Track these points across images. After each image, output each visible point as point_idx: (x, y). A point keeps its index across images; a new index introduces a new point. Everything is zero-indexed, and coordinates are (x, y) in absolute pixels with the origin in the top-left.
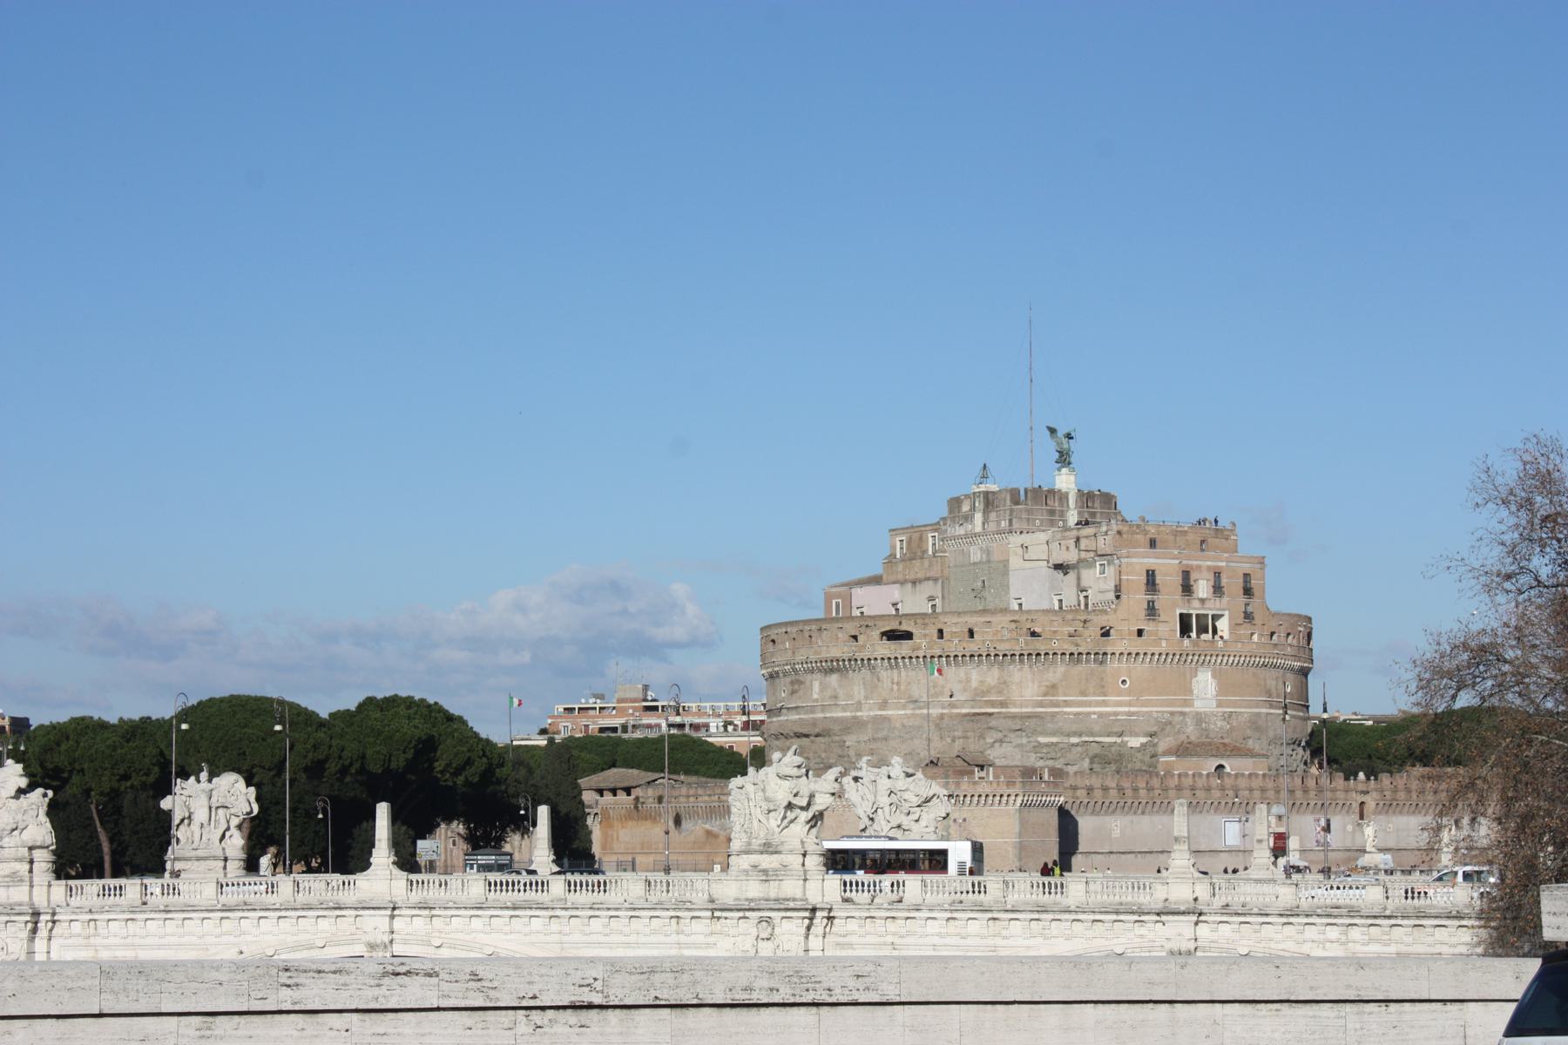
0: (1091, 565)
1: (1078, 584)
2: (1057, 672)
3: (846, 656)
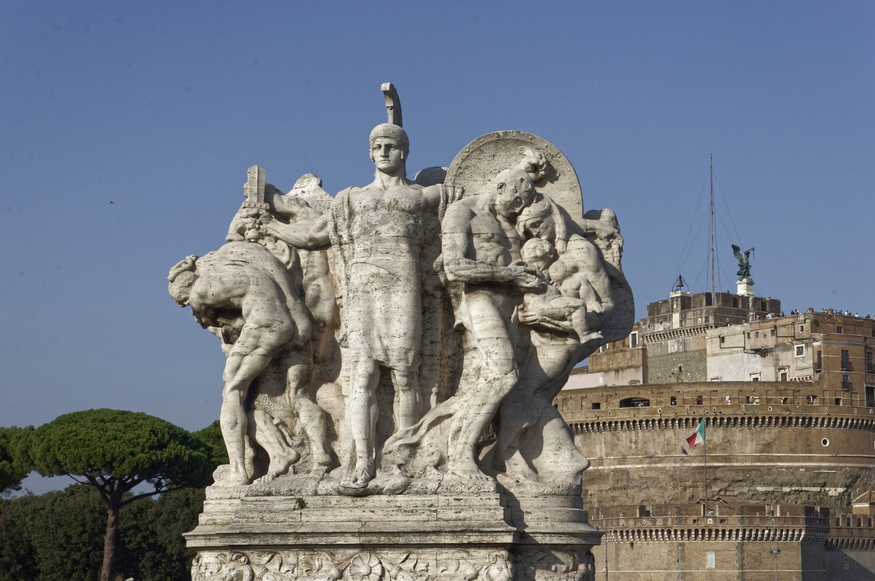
0: (787, 348)
1: (776, 366)
2: (771, 433)
3: (589, 420)
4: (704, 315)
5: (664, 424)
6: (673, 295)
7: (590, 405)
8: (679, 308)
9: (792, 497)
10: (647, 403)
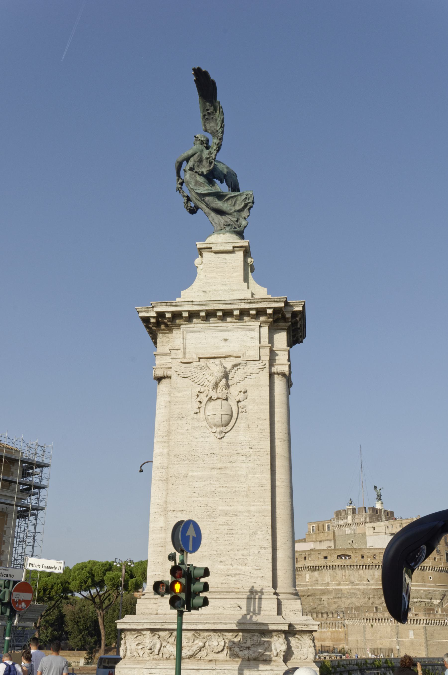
3: (322, 565)
4: (364, 517)
5: (358, 567)
6: (348, 507)
7: (323, 557)
8: (352, 513)
9: (418, 604)
10: (350, 556)
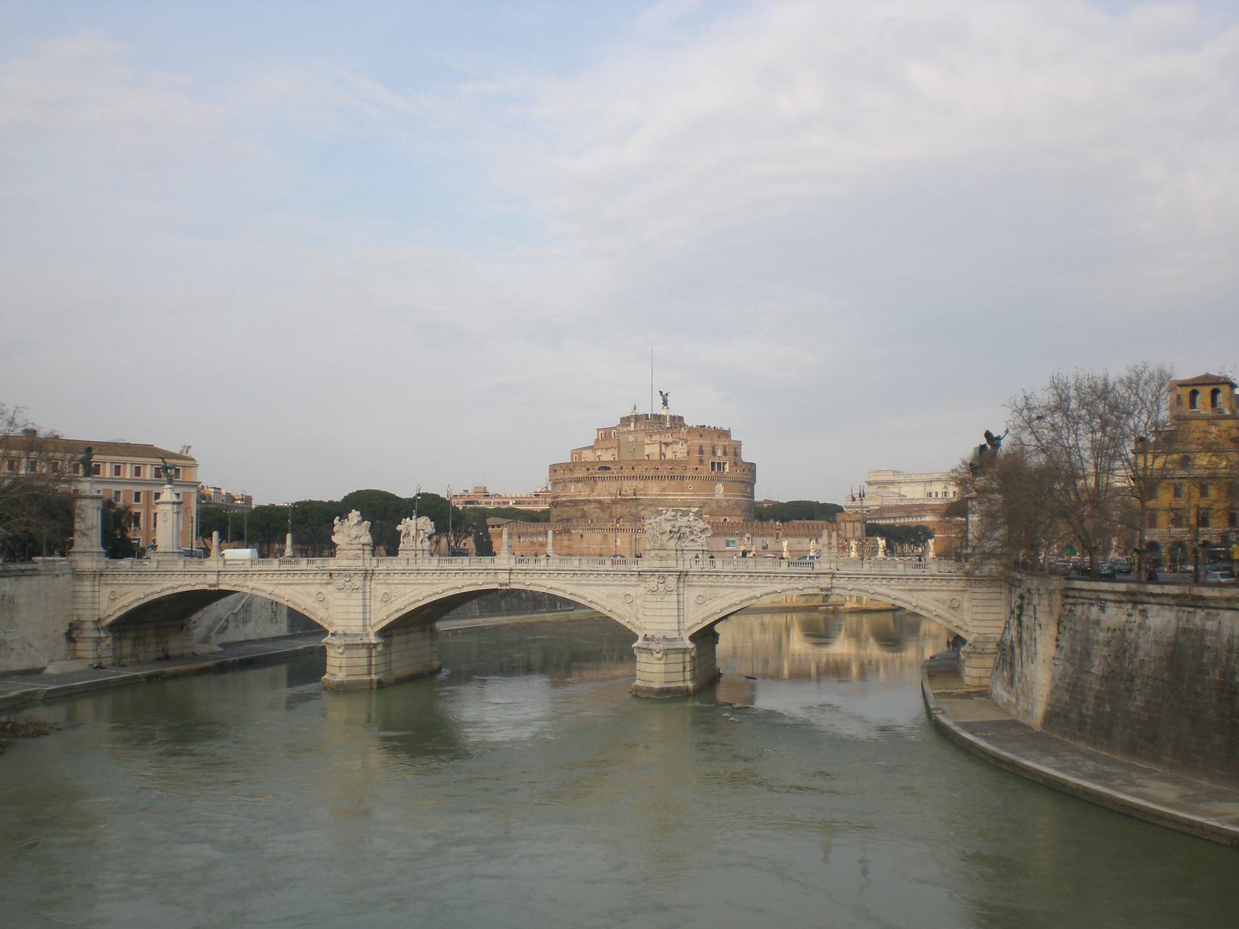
5: (617, 479)
